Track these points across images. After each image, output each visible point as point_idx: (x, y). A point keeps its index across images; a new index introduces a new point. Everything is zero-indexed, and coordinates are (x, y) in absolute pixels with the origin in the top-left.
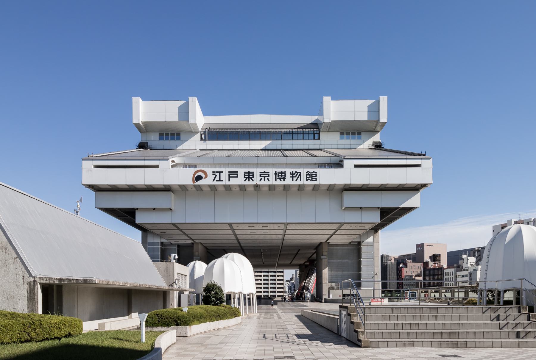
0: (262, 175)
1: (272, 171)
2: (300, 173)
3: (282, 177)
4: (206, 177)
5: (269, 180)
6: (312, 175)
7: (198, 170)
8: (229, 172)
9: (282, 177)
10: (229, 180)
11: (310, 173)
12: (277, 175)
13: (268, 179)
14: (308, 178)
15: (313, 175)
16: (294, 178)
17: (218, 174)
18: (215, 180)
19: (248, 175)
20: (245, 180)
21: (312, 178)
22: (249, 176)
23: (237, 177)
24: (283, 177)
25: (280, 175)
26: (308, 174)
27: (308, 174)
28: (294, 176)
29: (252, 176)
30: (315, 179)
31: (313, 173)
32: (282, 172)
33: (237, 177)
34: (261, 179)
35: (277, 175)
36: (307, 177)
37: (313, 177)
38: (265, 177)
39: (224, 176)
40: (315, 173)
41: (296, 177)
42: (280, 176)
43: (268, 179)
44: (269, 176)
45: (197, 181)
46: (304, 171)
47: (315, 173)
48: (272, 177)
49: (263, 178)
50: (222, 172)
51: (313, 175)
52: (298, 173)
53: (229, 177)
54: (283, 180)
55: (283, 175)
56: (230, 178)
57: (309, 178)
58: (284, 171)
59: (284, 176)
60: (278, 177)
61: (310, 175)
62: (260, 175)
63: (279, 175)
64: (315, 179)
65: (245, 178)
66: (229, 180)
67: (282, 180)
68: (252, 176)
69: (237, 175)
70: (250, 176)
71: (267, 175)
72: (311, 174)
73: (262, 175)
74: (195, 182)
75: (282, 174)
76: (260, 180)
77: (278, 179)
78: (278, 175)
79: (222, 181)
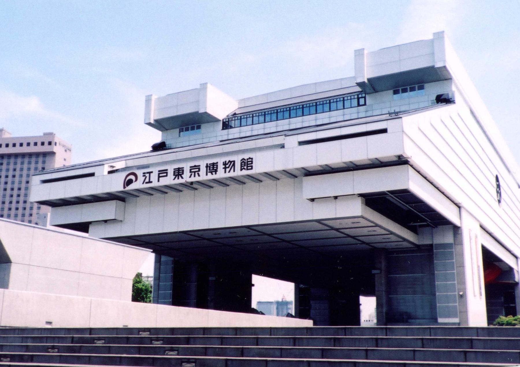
0: (192, 171)
2: (234, 161)
3: (213, 169)
4: (136, 180)
5: (199, 175)
6: (248, 162)
8: (159, 171)
10: (158, 181)
11: (245, 160)
12: (208, 168)
14: (242, 168)
15: (249, 163)
17: (147, 175)
19: (177, 172)
21: (247, 167)
22: (179, 172)
25: (212, 167)
27: (243, 162)
28: (227, 166)
29: (182, 173)
30: (250, 168)
31: (249, 160)
33: (166, 176)
34: (191, 175)
35: (208, 168)
36: (241, 166)
37: (249, 165)
38: (195, 172)
39: (154, 177)
40: (250, 160)
41: (228, 167)
44: (199, 171)
47: (250, 160)
49: (193, 173)
50: (152, 172)
51: (249, 163)
53: (159, 177)
60: (210, 170)
62: (191, 170)
64: (250, 168)
65: (175, 176)
66: (158, 181)
67: (214, 173)
68: (182, 173)
69: (167, 173)
71: (197, 170)
72: (246, 161)
73: (192, 171)
77: (209, 172)
78: (210, 168)
79: (151, 182)
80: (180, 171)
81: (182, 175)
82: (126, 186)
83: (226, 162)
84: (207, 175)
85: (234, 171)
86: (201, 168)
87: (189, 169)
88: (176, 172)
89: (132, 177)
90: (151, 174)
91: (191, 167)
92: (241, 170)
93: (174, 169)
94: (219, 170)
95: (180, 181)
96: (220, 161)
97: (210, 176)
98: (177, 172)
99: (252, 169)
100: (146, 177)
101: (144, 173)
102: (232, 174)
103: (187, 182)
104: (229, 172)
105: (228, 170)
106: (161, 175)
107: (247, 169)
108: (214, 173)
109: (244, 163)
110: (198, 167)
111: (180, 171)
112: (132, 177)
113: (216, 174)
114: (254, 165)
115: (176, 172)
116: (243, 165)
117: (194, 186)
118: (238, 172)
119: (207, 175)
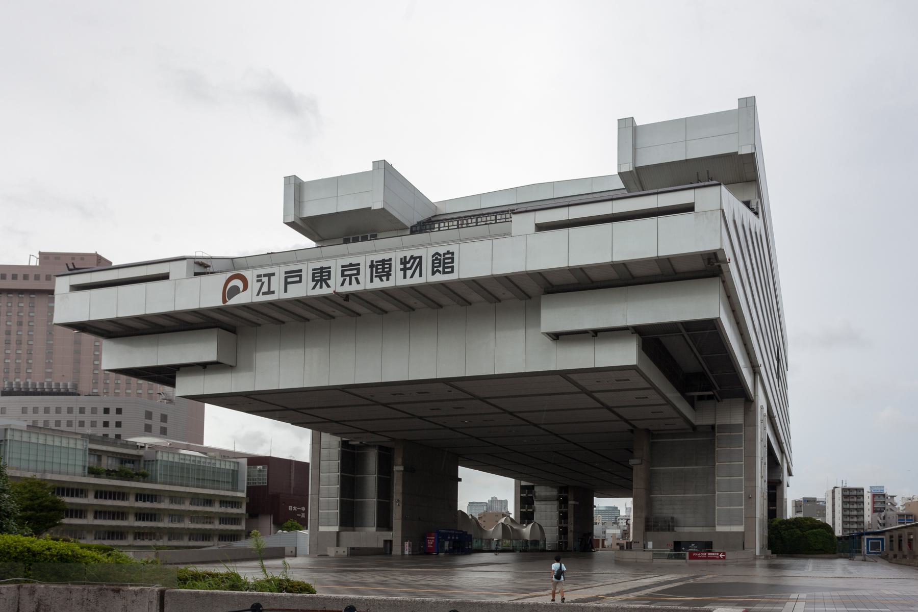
0: (346, 273)
1: (364, 262)
2: (420, 258)
3: (383, 271)
4: (245, 288)
5: (358, 283)
6: (444, 259)
8: (286, 273)
9: (383, 271)
10: (286, 291)
11: (440, 255)
12: (374, 269)
13: (357, 279)
14: (435, 269)
15: (446, 261)
16: (407, 271)
17: (265, 279)
18: (261, 294)
20: (314, 288)
21: (444, 268)
22: (321, 276)
23: (300, 281)
24: (385, 272)
25: (381, 267)
26: (437, 259)
28: (408, 266)
30: (450, 270)
31: (447, 256)
32: (384, 261)
33: (300, 281)
34: (344, 280)
35: (374, 269)
36: (433, 267)
37: (446, 265)
38: (350, 276)
40: (450, 256)
41: (410, 268)
42: (381, 270)
43: (357, 279)
44: (358, 274)
45: (229, 299)
47: (450, 256)
48: (365, 272)
49: (348, 278)
50: (273, 274)
51: (446, 261)
52: (415, 258)
53: (286, 283)
54: (386, 277)
55: (386, 266)
56: (288, 285)
57: (439, 268)
59: (388, 270)
60: (377, 272)
61: (440, 260)
62: (343, 272)
63: (379, 267)
64: (450, 270)
66: (286, 291)
67: (384, 278)
69: (300, 276)
70: (324, 278)
71: (355, 272)
73: (346, 273)
74: (227, 300)
75: (383, 265)
76: (342, 284)
77: (376, 276)
78: (377, 269)
79: (273, 292)
81: (327, 281)
82: (227, 300)
83: (405, 257)
84: (372, 281)
85: (421, 275)
86: (362, 268)
87: (340, 270)
89: (238, 283)
90: (272, 278)
91: (343, 267)
92: (433, 273)
93: (313, 270)
94: (393, 272)
95: (325, 291)
96: (396, 257)
97: (378, 284)
99: (452, 272)
100: (263, 283)
101: (259, 276)
102: (417, 280)
104: (412, 277)
105: (409, 273)
106: (289, 280)
107: (444, 273)
108: (384, 278)
109: (438, 261)
110: (356, 267)
112: (238, 283)
113: (388, 279)
114: (455, 264)
118: (428, 277)
119: (372, 281)
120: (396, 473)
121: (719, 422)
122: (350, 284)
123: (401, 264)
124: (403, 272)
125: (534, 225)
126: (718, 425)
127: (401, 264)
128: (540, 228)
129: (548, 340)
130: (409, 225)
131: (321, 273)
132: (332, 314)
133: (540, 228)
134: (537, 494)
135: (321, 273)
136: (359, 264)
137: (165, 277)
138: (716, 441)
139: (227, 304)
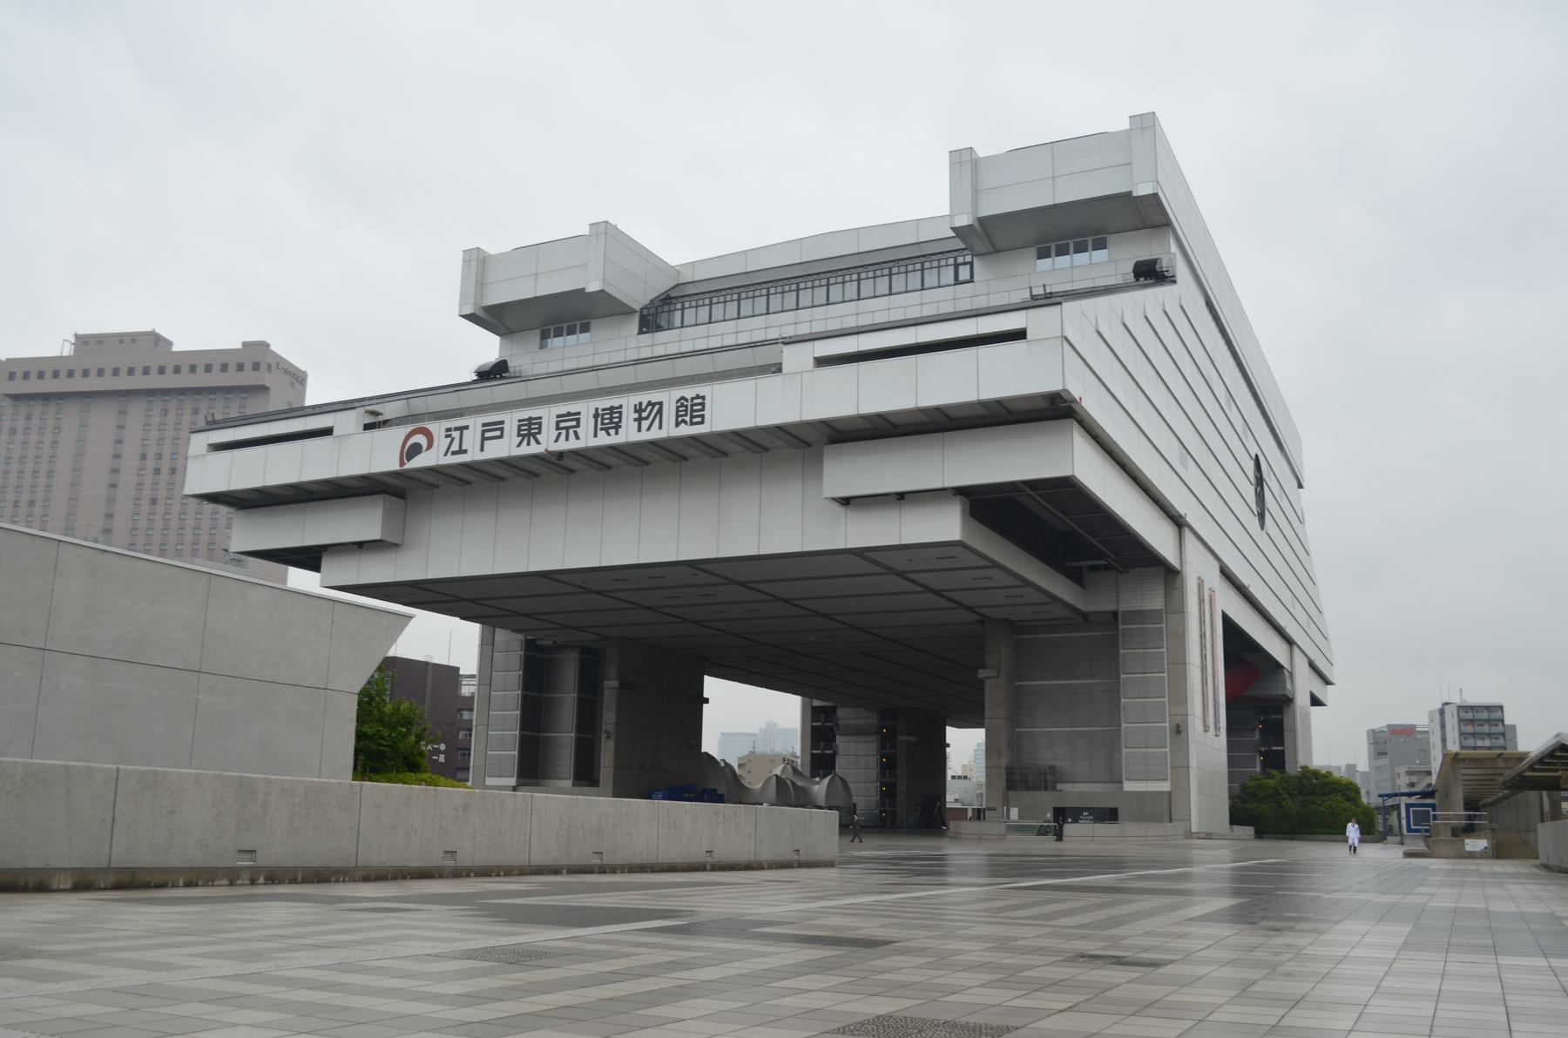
0: (562, 425)
2: (661, 404)
3: (611, 422)
4: (430, 446)
5: (577, 437)
6: (693, 405)
7: (414, 430)
8: (484, 425)
9: (611, 422)
10: (482, 450)
11: (686, 400)
12: (599, 419)
13: (576, 433)
14: (680, 419)
15: (695, 408)
17: (456, 434)
18: (450, 453)
19: (526, 427)
20: (519, 445)
21: (692, 417)
25: (608, 416)
26: (682, 405)
27: (682, 403)
30: (699, 419)
31: (696, 401)
32: (612, 408)
33: (501, 437)
34: (560, 434)
35: (599, 419)
36: (678, 416)
37: (695, 414)
38: (567, 428)
40: (700, 401)
41: (647, 418)
43: (576, 433)
44: (578, 426)
45: (408, 461)
46: (669, 398)
47: (700, 401)
49: (564, 432)
50: (467, 427)
51: (695, 408)
52: (653, 405)
53: (484, 439)
55: (615, 415)
56: (486, 442)
57: (685, 418)
58: (618, 405)
60: (602, 424)
61: (686, 406)
62: (558, 423)
64: (699, 419)
65: (520, 438)
66: (482, 450)
67: (612, 432)
69: (502, 430)
71: (574, 423)
72: (689, 404)
73: (562, 425)
75: (611, 414)
76: (556, 441)
77: (601, 429)
78: (603, 419)
80: (533, 427)
81: (538, 436)
83: (641, 404)
84: (595, 436)
85: (660, 428)
86: (583, 418)
87: (554, 420)
88: (523, 428)
89: (420, 439)
90: (465, 431)
91: (558, 416)
92: (678, 424)
93: (520, 421)
94: (623, 424)
95: (534, 449)
97: (604, 440)
98: (526, 427)
99: (702, 422)
100: (453, 439)
101: (448, 430)
102: (655, 434)
103: (550, 453)
104: (649, 429)
105: (645, 424)
106: (487, 435)
107: (692, 424)
108: (612, 432)
109: (684, 409)
110: (575, 417)
111: (533, 427)
112: (420, 439)
113: (617, 433)
114: (707, 413)
115: (523, 428)
116: (680, 413)
117: (567, 462)
119: (595, 436)
120: (607, 692)
121: (1125, 606)
122: (567, 439)
123: (635, 412)
124: (636, 423)
125: (812, 359)
126: (1123, 612)
127: (635, 412)
128: (822, 362)
129: (836, 506)
130: (637, 307)
131: (530, 424)
132: (537, 471)
133: (822, 362)
134: (840, 722)
135: (530, 424)
136: (579, 413)
137: (327, 432)
138: (1120, 637)
139: (405, 467)
